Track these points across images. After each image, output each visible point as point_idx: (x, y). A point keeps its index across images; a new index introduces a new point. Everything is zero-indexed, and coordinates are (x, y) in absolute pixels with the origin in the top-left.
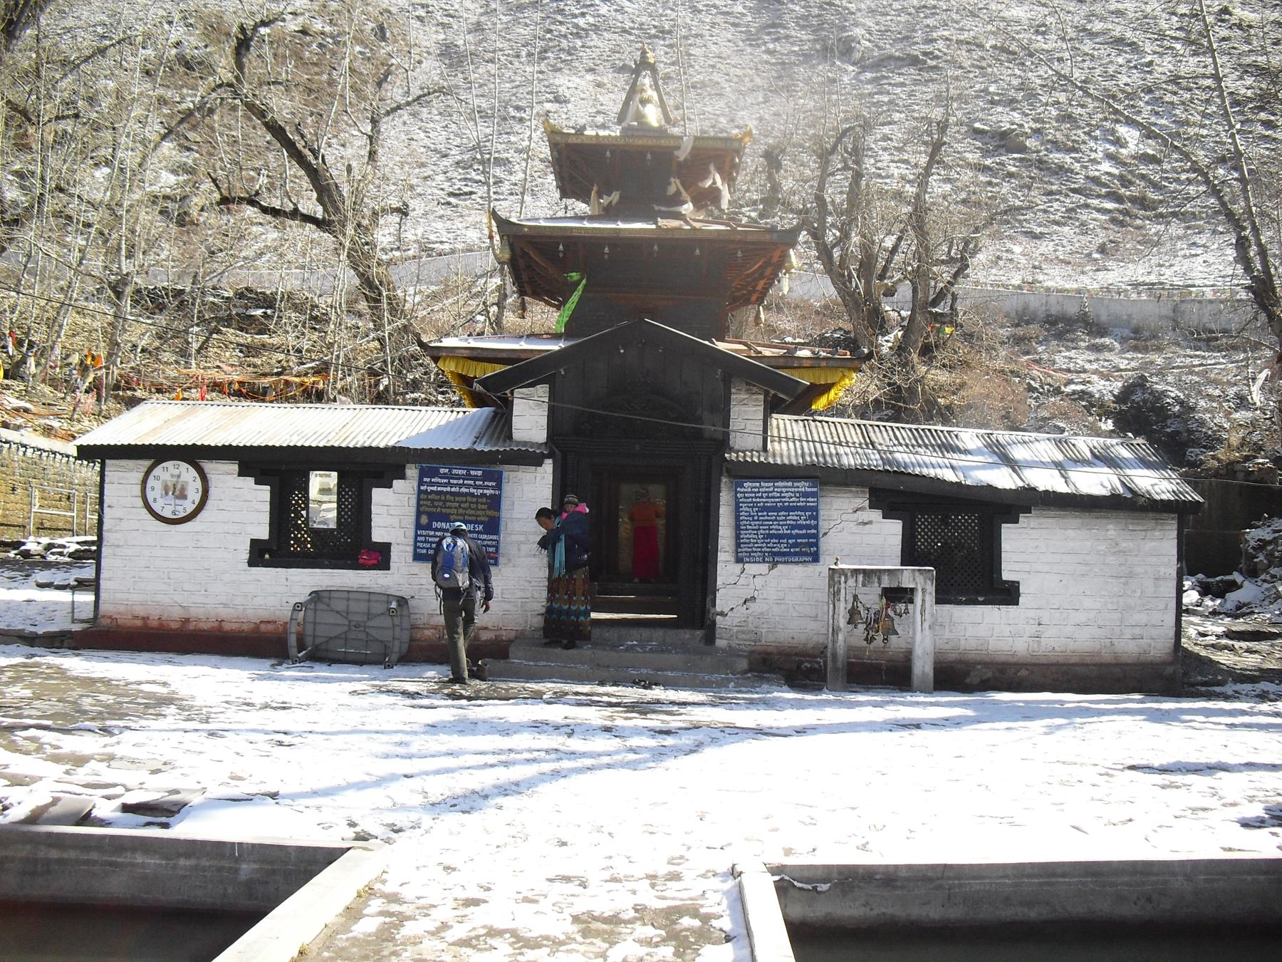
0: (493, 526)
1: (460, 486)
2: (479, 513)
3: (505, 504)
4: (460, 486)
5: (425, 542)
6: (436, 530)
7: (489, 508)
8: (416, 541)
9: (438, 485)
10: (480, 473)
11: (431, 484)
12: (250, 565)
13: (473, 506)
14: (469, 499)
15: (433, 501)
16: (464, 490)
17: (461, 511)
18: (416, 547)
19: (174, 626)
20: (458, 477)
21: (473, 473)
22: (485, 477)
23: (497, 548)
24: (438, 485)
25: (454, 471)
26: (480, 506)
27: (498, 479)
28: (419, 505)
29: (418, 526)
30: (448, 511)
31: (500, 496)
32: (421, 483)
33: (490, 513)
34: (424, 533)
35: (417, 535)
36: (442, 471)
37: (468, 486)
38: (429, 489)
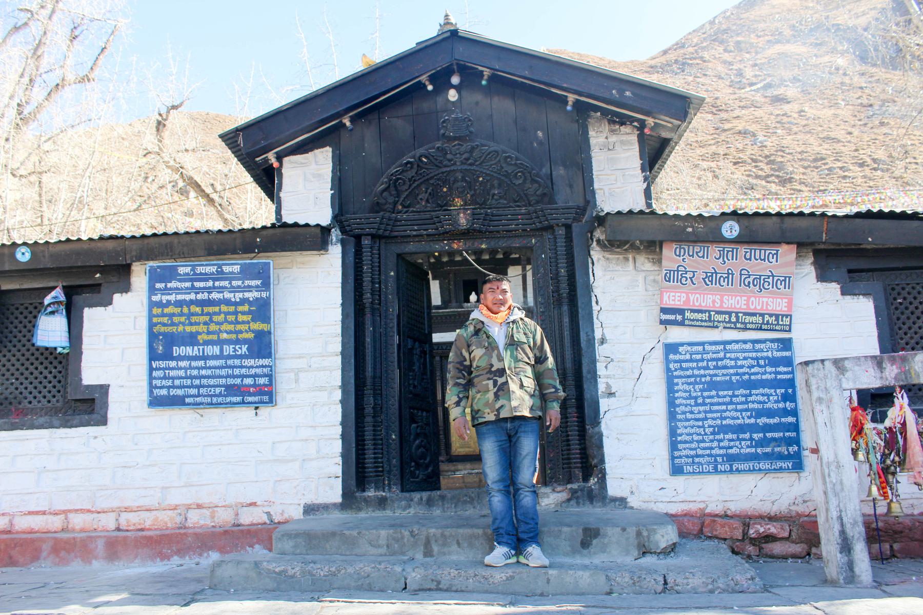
0: (262, 346)
1: (209, 290)
2: (239, 327)
4: (209, 290)
5: (165, 378)
6: (180, 358)
7: (253, 320)
8: (151, 378)
13: (231, 318)
14: (224, 308)
16: (215, 296)
17: (213, 327)
18: (152, 388)
20: (204, 277)
21: (226, 269)
22: (246, 272)
23: (270, 376)
24: (178, 291)
25: (200, 270)
26: (241, 318)
28: (151, 325)
30: (194, 329)
31: (269, 298)
32: (152, 290)
33: (257, 326)
34: (162, 364)
35: (151, 369)
37: (221, 289)
38: (165, 298)
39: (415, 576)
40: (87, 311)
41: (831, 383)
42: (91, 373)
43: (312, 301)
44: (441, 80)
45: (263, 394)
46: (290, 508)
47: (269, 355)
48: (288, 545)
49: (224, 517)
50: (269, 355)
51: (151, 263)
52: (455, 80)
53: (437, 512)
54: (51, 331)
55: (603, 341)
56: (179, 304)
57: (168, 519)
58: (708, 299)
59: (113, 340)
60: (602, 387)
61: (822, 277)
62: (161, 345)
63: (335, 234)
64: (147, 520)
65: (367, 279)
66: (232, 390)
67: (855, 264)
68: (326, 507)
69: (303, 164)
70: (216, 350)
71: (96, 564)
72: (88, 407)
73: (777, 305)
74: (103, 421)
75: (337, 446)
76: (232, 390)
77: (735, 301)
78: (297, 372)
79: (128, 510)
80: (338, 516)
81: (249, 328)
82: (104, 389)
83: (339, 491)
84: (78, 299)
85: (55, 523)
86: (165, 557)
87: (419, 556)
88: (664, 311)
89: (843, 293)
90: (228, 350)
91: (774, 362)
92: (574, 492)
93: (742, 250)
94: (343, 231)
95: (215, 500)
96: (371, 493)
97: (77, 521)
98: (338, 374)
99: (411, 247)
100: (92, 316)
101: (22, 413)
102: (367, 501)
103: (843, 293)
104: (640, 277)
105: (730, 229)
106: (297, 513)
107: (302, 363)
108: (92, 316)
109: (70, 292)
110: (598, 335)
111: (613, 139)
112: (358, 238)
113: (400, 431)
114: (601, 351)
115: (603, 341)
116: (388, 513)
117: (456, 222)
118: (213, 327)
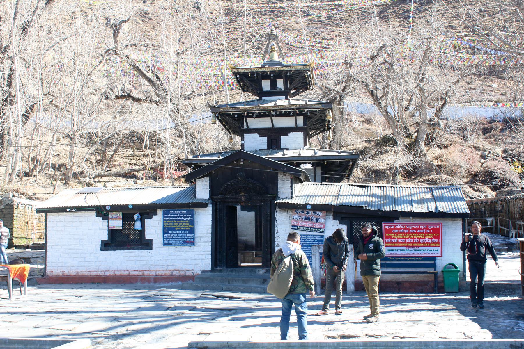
0: (192, 231)
1: (178, 217)
3: (195, 223)
4: (178, 217)
8: (164, 238)
9: (170, 217)
10: (185, 212)
11: (167, 217)
12: (102, 250)
15: (169, 223)
16: (180, 218)
17: (179, 226)
18: (164, 241)
19: (74, 274)
22: (188, 213)
23: (194, 239)
24: (170, 217)
25: (176, 212)
27: (192, 213)
28: (164, 225)
29: (164, 233)
32: (164, 217)
33: (190, 226)
34: (167, 235)
35: (164, 236)
36: (171, 212)
39: (224, 287)
40: (146, 220)
41: (316, 251)
42: (148, 237)
43: (204, 220)
44: (238, 160)
45: (192, 243)
46: (198, 271)
47: (193, 233)
48: (198, 280)
49: (182, 273)
50: (193, 233)
51: (164, 210)
52: (242, 160)
53: (234, 274)
54: (138, 225)
55: (277, 232)
56: (171, 220)
57: (168, 273)
58: (303, 224)
59: (154, 228)
60: (276, 244)
61: (334, 219)
62: (166, 230)
63: (210, 201)
64: (163, 273)
65: (218, 213)
66: (184, 242)
67: (343, 216)
68: (207, 271)
69: (202, 181)
70: (180, 232)
71: (151, 284)
72: (147, 245)
73: (321, 226)
74: (151, 249)
75: (210, 256)
76: (184, 242)
77: (310, 225)
78: (200, 237)
79: (159, 271)
80: (210, 274)
81: (188, 227)
82: (151, 240)
83: (210, 267)
84: (143, 216)
85: (140, 273)
86: (168, 282)
87: (227, 284)
88: (292, 226)
89: (340, 223)
90: (183, 232)
91: (318, 241)
92: (267, 270)
93: (313, 212)
94: (212, 200)
95: (180, 269)
96: (218, 268)
97: (146, 273)
98: (211, 238)
99: (230, 204)
100: (147, 221)
101: (130, 245)
102: (217, 270)
103: (340, 223)
104: (288, 216)
105: (309, 207)
106: (200, 273)
107: (201, 235)
108: (147, 221)
109: (140, 214)
110: (276, 231)
111: (284, 177)
112: (216, 202)
113: (228, 251)
114: (277, 235)
115: (277, 232)
116: (222, 273)
117: (241, 199)
118: (179, 226)
